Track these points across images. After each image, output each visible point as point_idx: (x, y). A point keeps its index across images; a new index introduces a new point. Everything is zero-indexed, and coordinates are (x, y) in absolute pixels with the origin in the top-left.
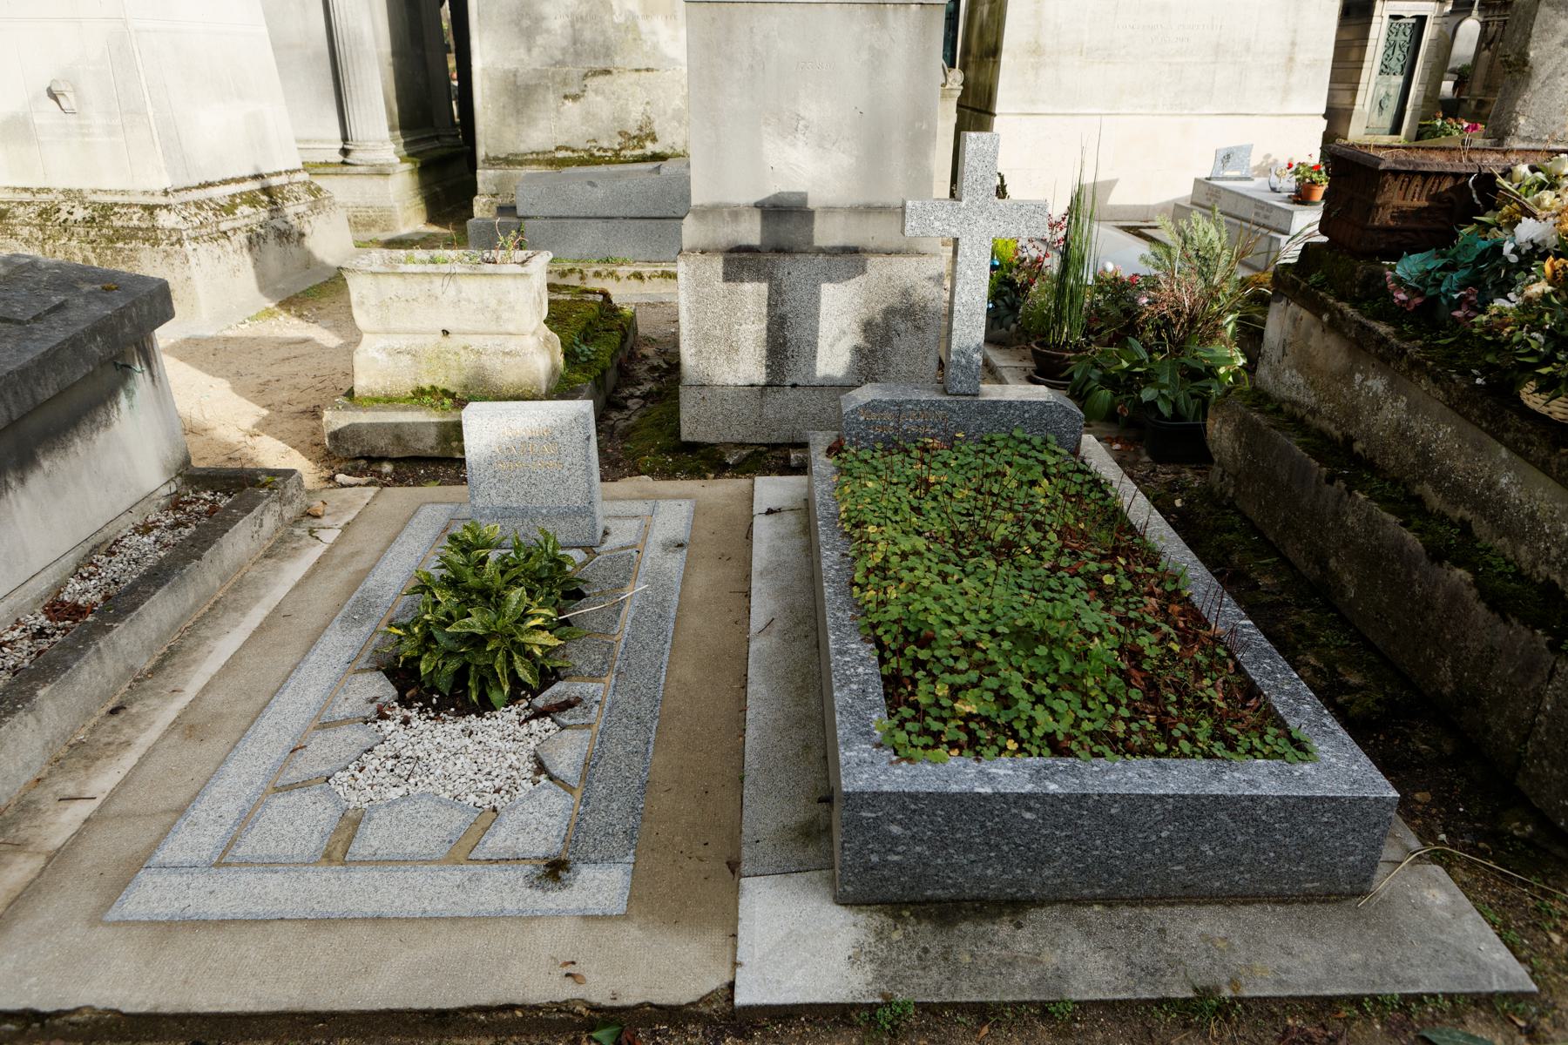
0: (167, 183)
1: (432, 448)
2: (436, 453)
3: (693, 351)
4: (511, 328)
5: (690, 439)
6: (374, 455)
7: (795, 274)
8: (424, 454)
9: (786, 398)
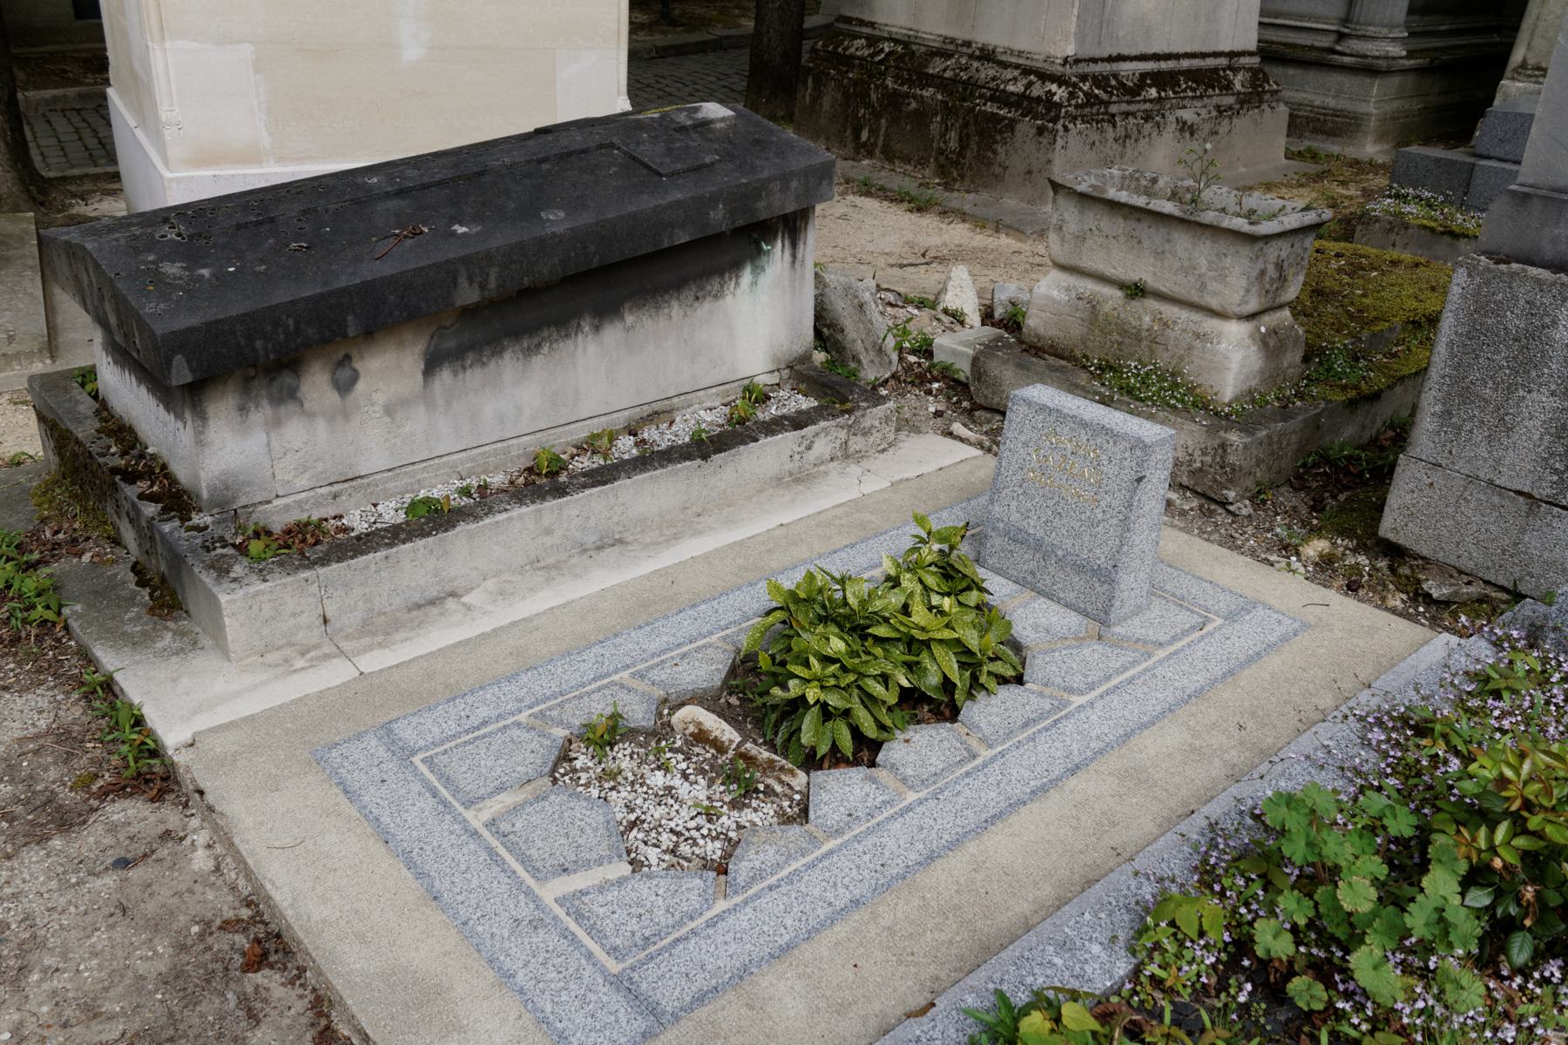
0: (1070, 50)
3: (1438, 408)
4: (1214, 303)
5: (1391, 536)
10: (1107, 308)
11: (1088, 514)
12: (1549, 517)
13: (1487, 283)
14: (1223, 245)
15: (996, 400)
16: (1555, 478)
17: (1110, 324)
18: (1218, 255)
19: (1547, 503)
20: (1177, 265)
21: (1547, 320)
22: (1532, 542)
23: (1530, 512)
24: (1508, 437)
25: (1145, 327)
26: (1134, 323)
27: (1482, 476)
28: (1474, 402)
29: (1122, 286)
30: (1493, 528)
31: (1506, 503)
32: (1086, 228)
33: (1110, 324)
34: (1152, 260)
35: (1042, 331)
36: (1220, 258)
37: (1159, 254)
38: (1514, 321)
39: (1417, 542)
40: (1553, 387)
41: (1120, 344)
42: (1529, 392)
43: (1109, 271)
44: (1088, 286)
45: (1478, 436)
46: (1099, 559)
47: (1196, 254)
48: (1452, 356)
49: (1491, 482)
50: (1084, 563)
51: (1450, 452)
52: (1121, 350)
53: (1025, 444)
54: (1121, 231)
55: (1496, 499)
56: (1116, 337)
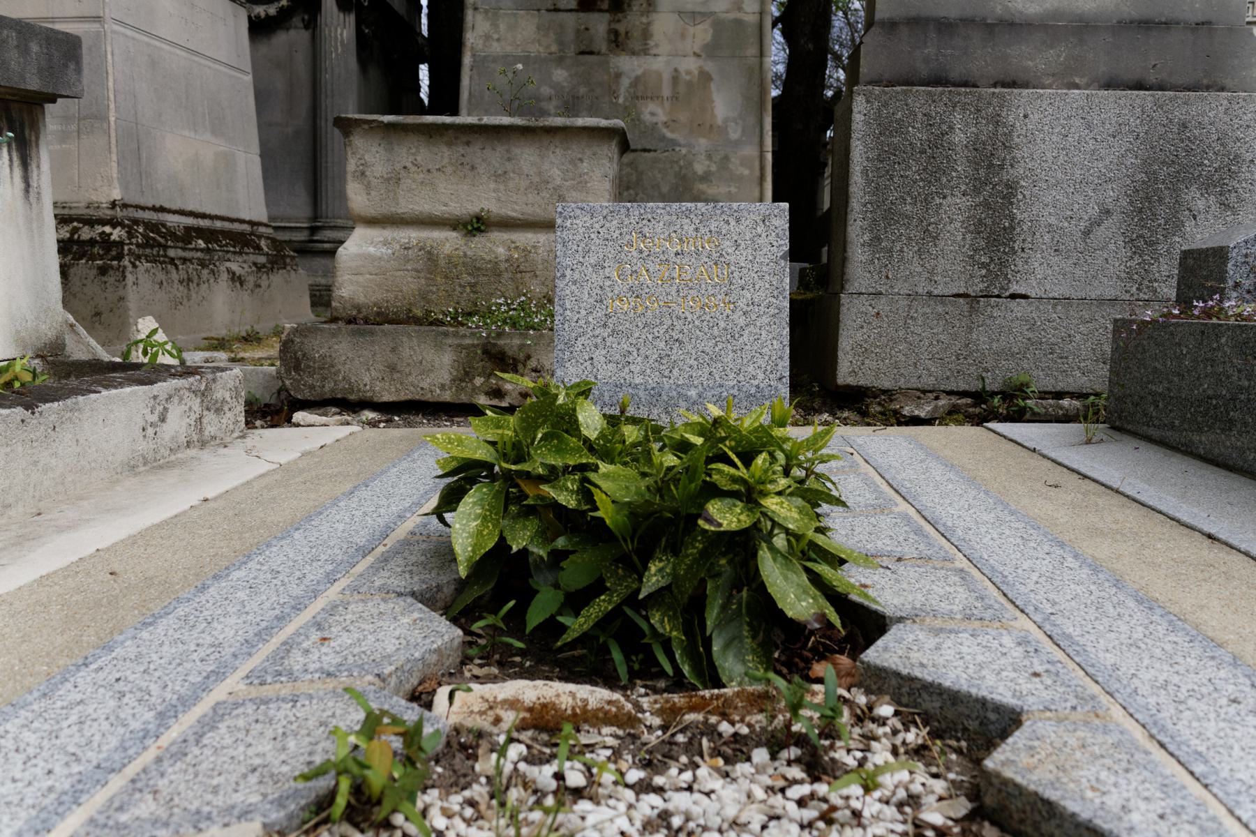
0: (116, 194)
1: (443, 387)
2: (447, 396)
3: (866, 237)
5: (851, 381)
6: (352, 397)
7: (1035, 117)
8: (428, 397)
9: (1009, 316)
10: (447, 249)
11: (722, 324)
12: (989, 309)
13: (886, 105)
14: (575, 150)
15: (329, 386)
16: (984, 272)
17: (456, 266)
18: (572, 162)
19: (982, 297)
20: (524, 183)
21: (944, 127)
22: (981, 338)
23: (973, 310)
24: (936, 245)
25: (503, 258)
26: (488, 258)
27: (920, 290)
28: (898, 222)
29: (454, 224)
30: (942, 337)
31: (949, 308)
32: (398, 167)
33: (456, 266)
34: (492, 186)
35: (361, 299)
36: (575, 165)
37: (501, 177)
38: (917, 134)
39: (877, 377)
40: (963, 187)
41: (472, 286)
42: (945, 197)
43: (438, 210)
44: (413, 235)
45: (909, 254)
46: (754, 377)
47: (546, 166)
48: (869, 182)
49: (930, 294)
50: (735, 392)
51: (887, 277)
52: (475, 292)
53: (598, 266)
54: (446, 161)
55: (940, 309)
56: (467, 278)
